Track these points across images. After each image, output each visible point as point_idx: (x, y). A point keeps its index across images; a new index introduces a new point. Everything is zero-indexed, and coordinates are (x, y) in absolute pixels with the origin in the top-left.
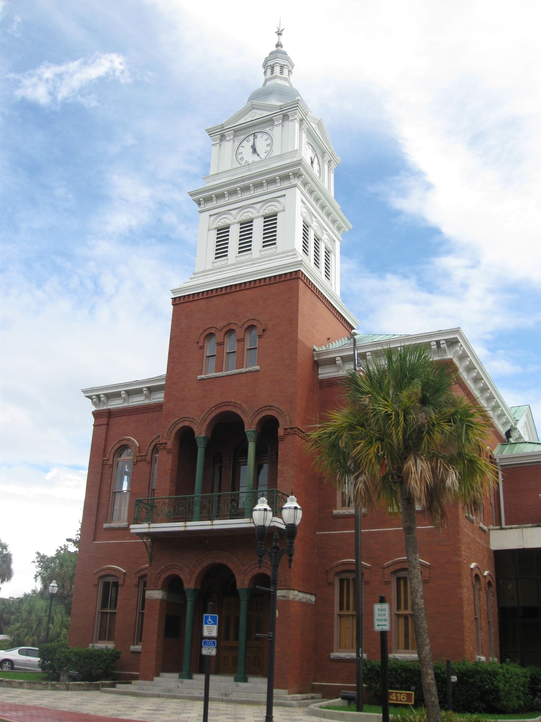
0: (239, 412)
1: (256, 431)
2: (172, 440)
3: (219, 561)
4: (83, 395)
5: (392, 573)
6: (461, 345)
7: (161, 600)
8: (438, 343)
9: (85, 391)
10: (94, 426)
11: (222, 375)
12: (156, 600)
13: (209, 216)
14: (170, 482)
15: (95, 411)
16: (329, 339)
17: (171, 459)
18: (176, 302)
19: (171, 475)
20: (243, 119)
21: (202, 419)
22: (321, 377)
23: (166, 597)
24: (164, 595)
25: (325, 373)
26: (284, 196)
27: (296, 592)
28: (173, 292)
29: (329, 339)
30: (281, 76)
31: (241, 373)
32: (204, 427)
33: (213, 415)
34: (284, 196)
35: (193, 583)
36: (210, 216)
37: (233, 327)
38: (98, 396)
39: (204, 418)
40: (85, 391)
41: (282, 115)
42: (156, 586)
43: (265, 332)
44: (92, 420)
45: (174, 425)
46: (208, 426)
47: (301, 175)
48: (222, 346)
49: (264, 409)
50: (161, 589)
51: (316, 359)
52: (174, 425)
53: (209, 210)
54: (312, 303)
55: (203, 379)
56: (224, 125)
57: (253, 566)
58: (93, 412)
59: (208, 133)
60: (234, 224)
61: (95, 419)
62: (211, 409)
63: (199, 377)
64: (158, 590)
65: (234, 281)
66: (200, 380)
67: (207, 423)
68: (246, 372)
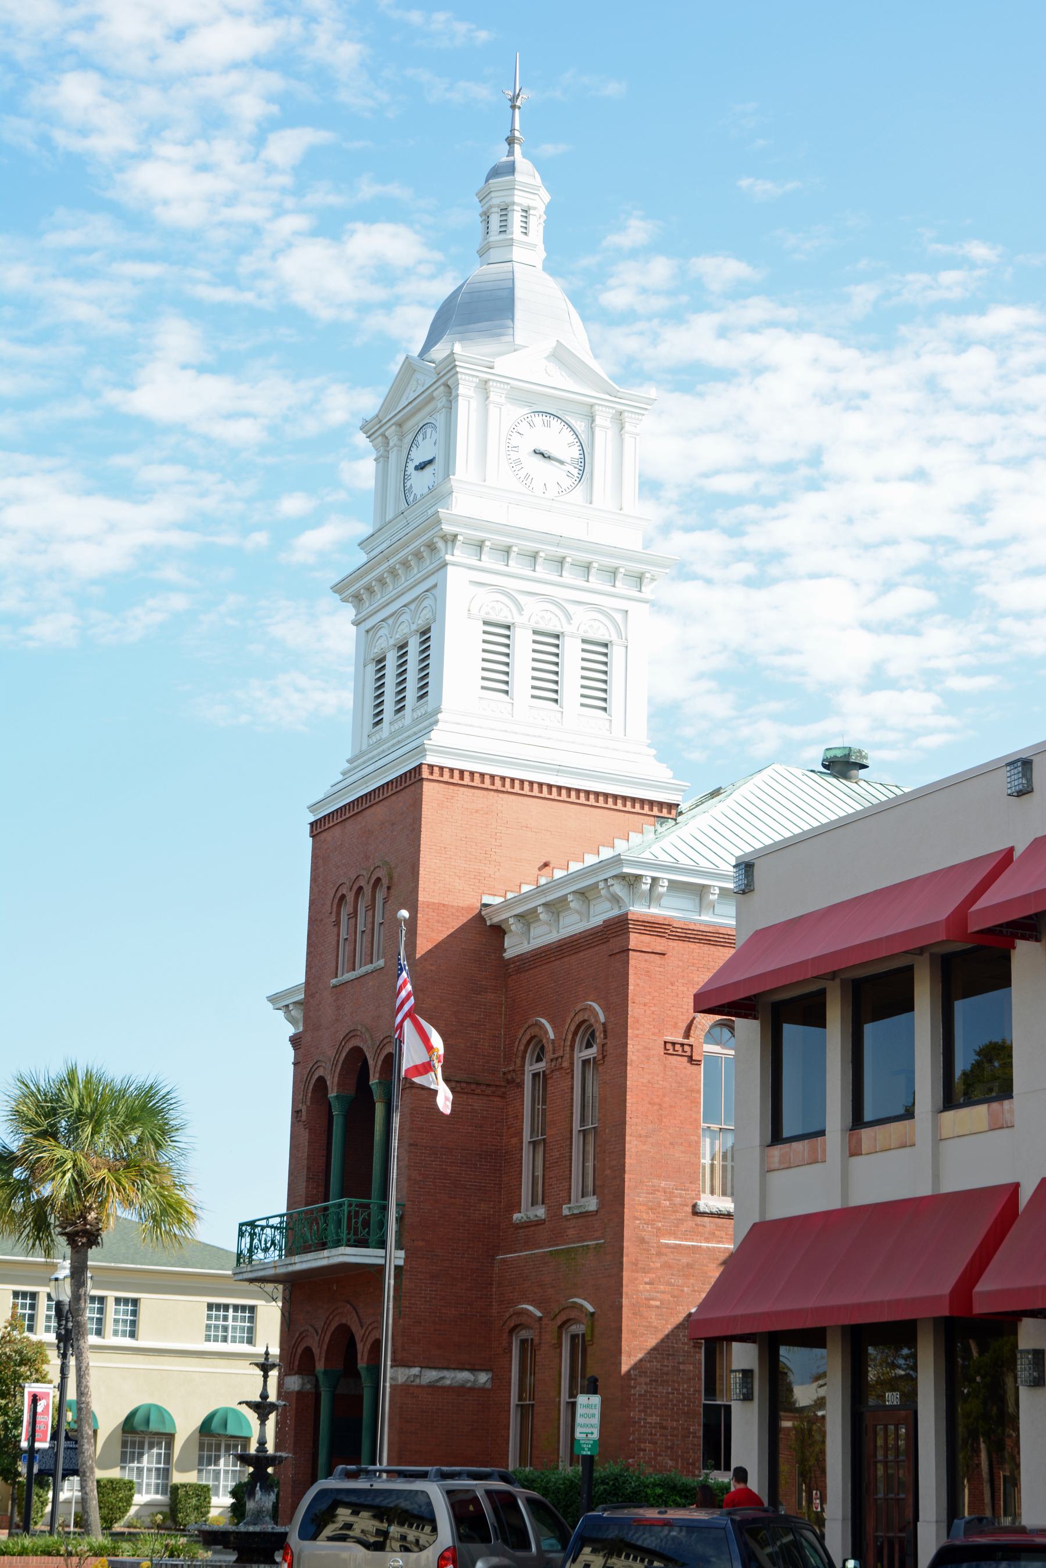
0: (365, 1049)
1: (380, 1083)
2: (308, 1104)
3: (344, 1321)
4: (270, 1006)
5: (560, 1327)
6: (654, 880)
7: (299, 1393)
8: (606, 880)
9: (273, 999)
10: (295, 1064)
11: (352, 978)
12: (292, 1392)
13: (364, 633)
14: (307, 1181)
15: (295, 1035)
16: (546, 865)
17: (307, 1138)
18: (317, 828)
19: (308, 1168)
20: (404, 398)
21: (333, 1063)
22: (507, 955)
23: (308, 1386)
24: (303, 1384)
25: (515, 946)
26: (435, 586)
27: (415, 1371)
28: (312, 808)
29: (546, 865)
30: (503, 236)
31: (367, 974)
32: (336, 1079)
33: (344, 1054)
34: (435, 586)
35: (323, 1359)
36: (367, 632)
37: (362, 883)
38: (287, 1006)
39: (335, 1062)
40: (273, 999)
41: (442, 388)
42: (293, 1369)
43: (392, 891)
44: (289, 1053)
45: (310, 1075)
46: (340, 1075)
47: (456, 536)
48: (354, 920)
49: (385, 1042)
50: (299, 1374)
51: (488, 923)
52: (310, 1075)
53: (365, 620)
54: (477, 811)
55: (335, 987)
56: (379, 416)
57: (370, 1328)
58: (290, 1037)
59: (366, 433)
60: (411, 635)
61: (295, 1050)
62: (341, 1043)
63: (334, 981)
64: (295, 1374)
65: (365, 786)
66: (333, 987)
67: (338, 1071)
68: (372, 972)
